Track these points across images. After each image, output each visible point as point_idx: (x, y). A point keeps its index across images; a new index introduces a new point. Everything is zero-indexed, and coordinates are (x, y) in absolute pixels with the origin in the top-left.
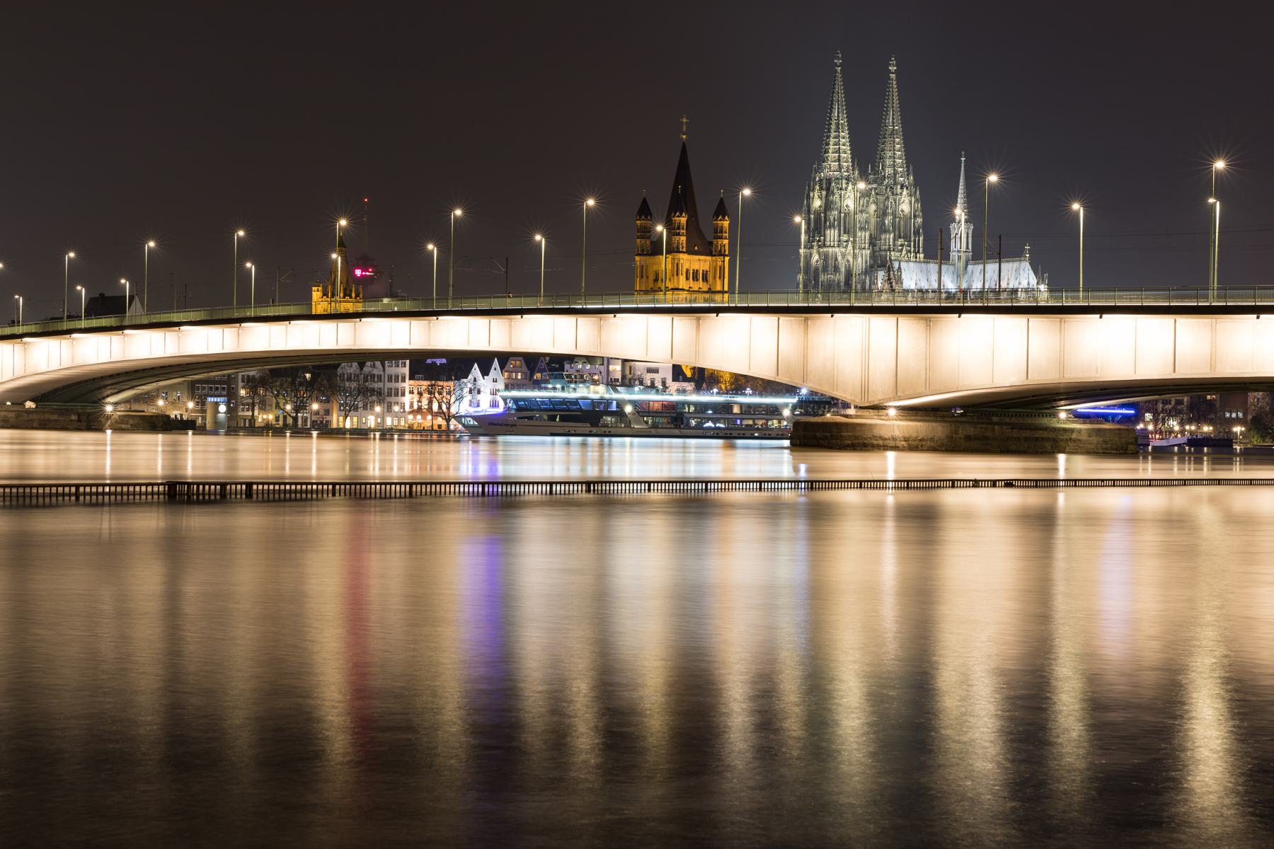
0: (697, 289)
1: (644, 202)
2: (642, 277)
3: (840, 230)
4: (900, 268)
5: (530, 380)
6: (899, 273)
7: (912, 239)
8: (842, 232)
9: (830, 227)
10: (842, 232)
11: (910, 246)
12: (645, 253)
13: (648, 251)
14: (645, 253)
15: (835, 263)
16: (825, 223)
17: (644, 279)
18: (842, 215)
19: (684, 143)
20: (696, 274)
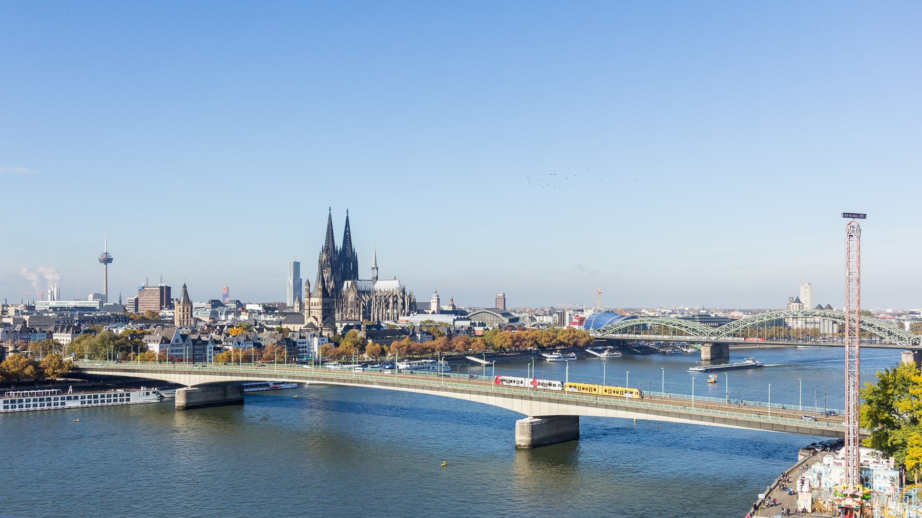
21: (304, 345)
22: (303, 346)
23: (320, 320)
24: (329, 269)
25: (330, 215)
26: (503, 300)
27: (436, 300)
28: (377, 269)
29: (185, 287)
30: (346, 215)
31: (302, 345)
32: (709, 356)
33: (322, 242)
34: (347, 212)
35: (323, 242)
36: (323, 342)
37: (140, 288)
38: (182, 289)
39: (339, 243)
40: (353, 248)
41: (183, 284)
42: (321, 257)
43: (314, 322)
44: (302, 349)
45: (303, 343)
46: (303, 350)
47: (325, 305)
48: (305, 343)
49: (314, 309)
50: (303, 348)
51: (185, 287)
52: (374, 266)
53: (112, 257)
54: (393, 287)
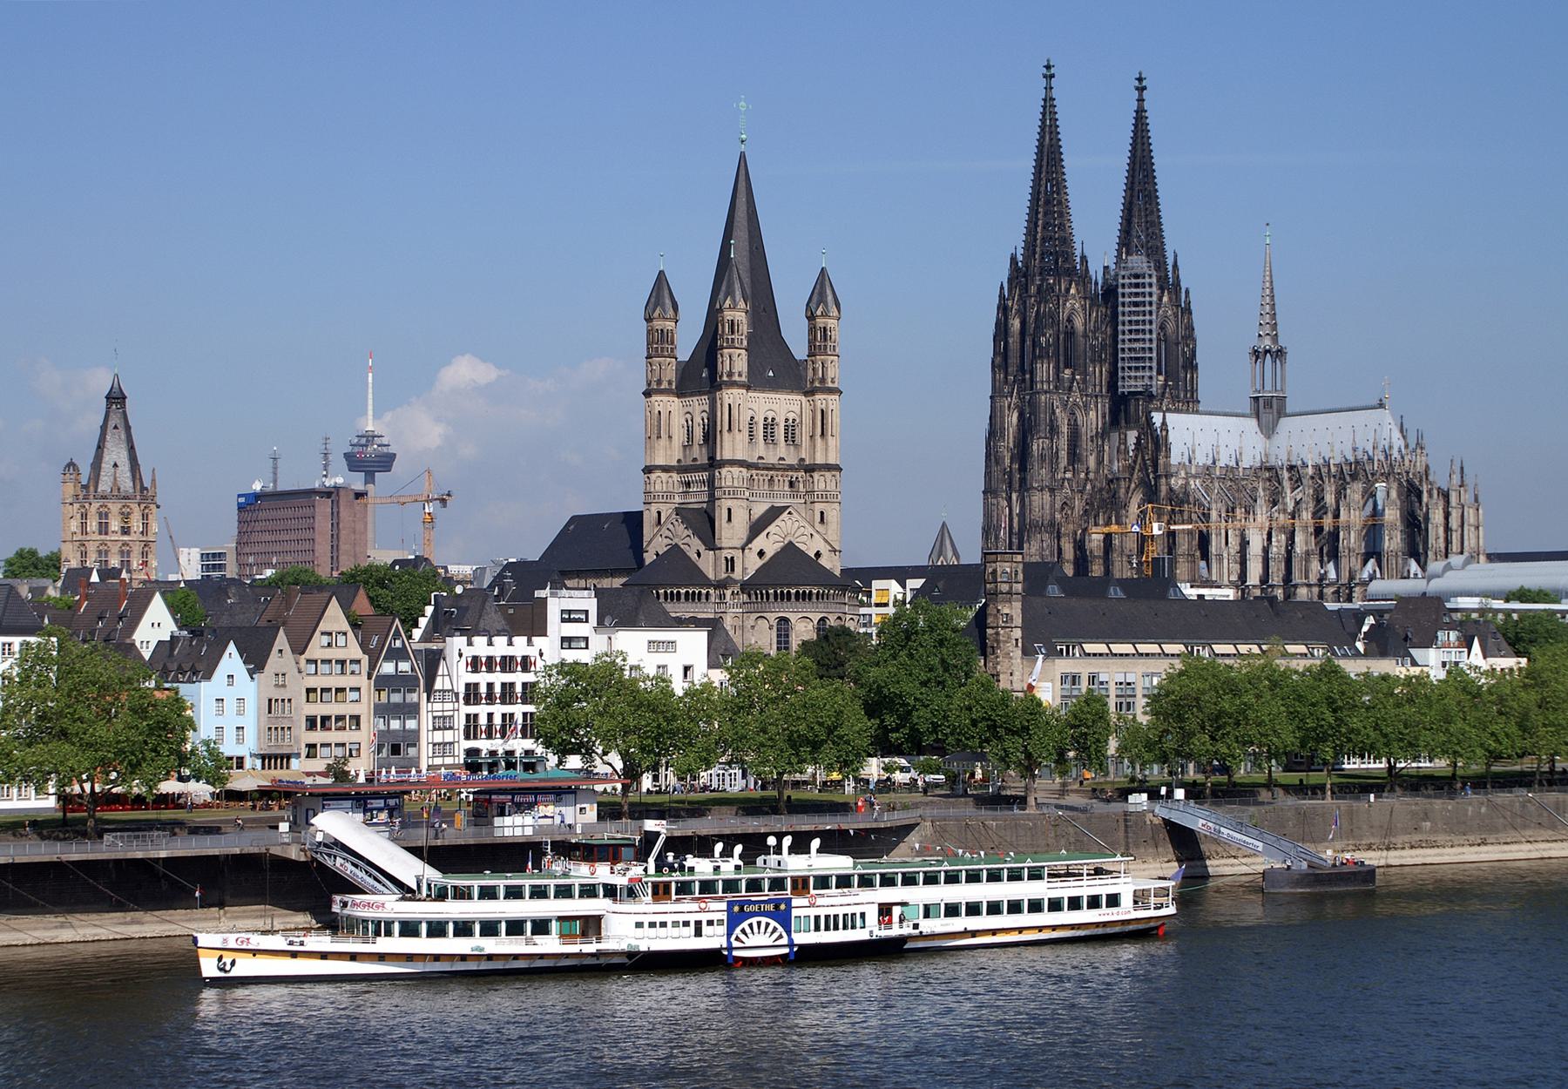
0: (772, 459)
1: (661, 277)
2: (659, 437)
3: (1058, 362)
4: (1164, 423)
5: (369, 677)
6: (1164, 433)
7: (1182, 375)
8: (1062, 365)
9: (1041, 357)
10: (1062, 365)
11: (1176, 387)
12: (664, 385)
13: (670, 383)
14: (664, 385)
15: (1051, 420)
16: (1034, 350)
17: (664, 441)
18: (1061, 337)
19: (743, 156)
21: (519, 678)
22: (508, 688)
25: (1049, 105)
28: (1279, 354)
30: (1135, 106)
31: (498, 678)
34: (1141, 89)
35: (1013, 238)
36: (662, 658)
37: (242, 500)
40: (1170, 268)
42: (1003, 309)
44: (499, 710)
45: (507, 664)
46: (508, 718)
47: (769, 435)
48: (526, 664)
52: (1267, 342)
53: (391, 450)
54: (1360, 445)
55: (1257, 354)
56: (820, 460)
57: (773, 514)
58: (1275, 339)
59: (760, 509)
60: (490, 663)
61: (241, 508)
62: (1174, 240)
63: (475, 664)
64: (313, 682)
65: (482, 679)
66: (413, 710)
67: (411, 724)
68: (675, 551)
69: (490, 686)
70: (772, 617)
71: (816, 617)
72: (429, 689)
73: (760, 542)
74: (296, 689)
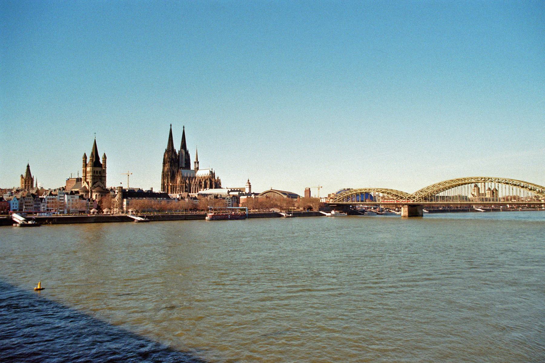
20: (97, 172)
21: (53, 201)
23: (90, 184)
24: (169, 164)
26: (309, 192)
27: (248, 186)
28: (198, 163)
29: (28, 166)
31: (51, 201)
32: (407, 214)
33: (165, 146)
38: (26, 168)
39: (177, 147)
41: (27, 165)
42: (165, 156)
43: (87, 186)
45: (53, 199)
47: (97, 173)
49: (88, 176)
50: (53, 202)
51: (28, 166)
55: (195, 163)
56: (103, 175)
57: (97, 182)
58: (197, 161)
59: (96, 181)
60: (50, 199)
61: (67, 181)
62: (188, 148)
63: (48, 199)
64: (26, 201)
65: (49, 201)
66: (40, 204)
67: (39, 206)
68: (85, 187)
69: (50, 202)
70: (95, 194)
71: (101, 194)
72: (42, 202)
73: (95, 185)
74: (23, 201)
